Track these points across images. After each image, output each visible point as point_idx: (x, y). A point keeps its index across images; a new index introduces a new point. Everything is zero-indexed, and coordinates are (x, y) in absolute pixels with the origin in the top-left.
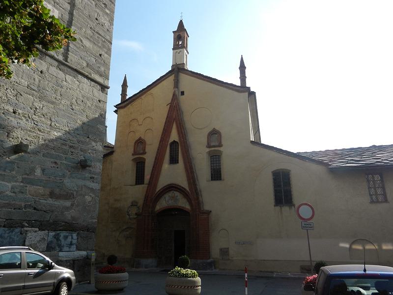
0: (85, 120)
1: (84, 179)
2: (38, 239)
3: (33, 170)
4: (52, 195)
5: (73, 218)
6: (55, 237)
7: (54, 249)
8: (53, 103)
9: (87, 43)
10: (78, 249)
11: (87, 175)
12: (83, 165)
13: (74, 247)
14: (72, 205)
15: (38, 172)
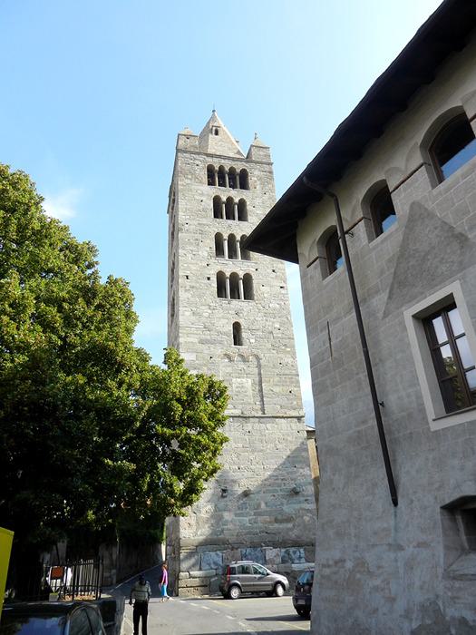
0: (289, 453)
1: (300, 502)
2: (274, 554)
3: (259, 505)
4: (276, 521)
5: (298, 537)
6: (286, 552)
7: (287, 562)
8: (261, 451)
9: (277, 389)
10: (307, 561)
11: (302, 499)
12: (295, 492)
13: (303, 560)
14: (294, 526)
15: (263, 505)
